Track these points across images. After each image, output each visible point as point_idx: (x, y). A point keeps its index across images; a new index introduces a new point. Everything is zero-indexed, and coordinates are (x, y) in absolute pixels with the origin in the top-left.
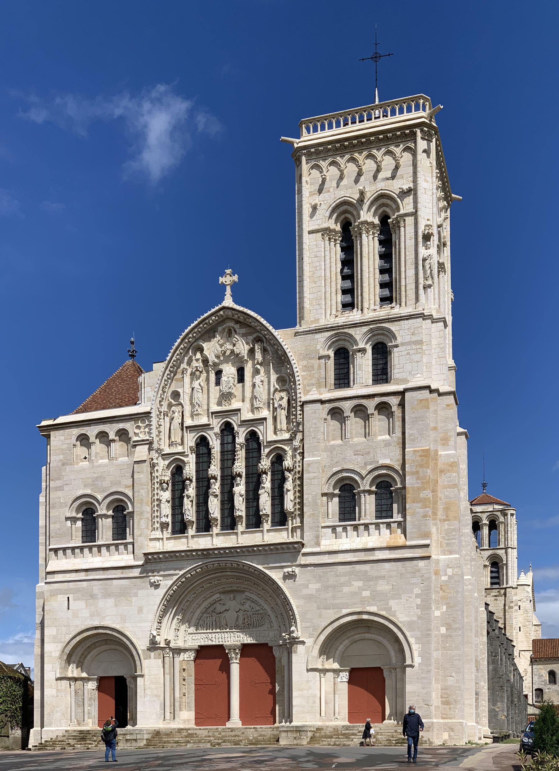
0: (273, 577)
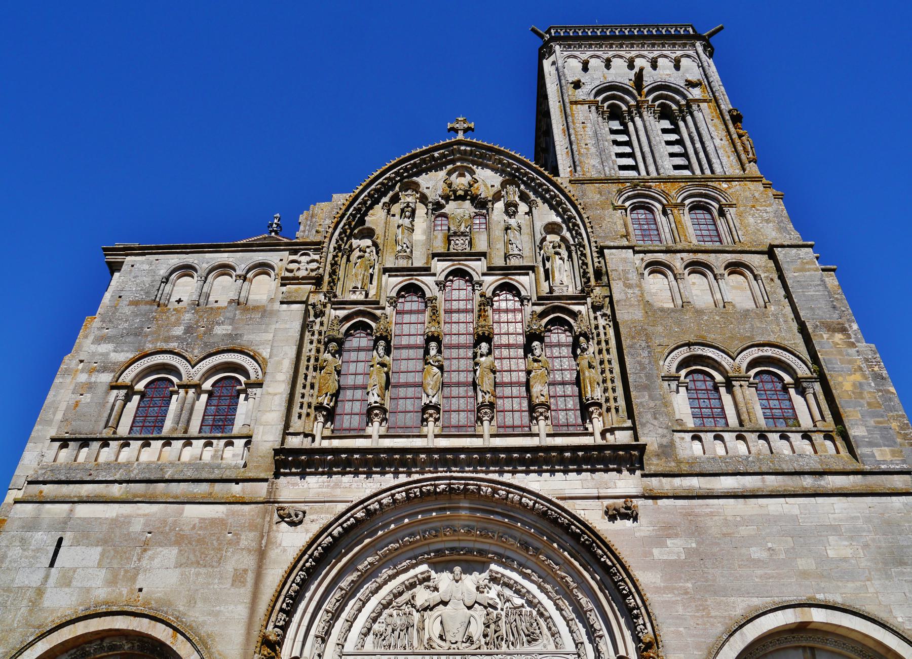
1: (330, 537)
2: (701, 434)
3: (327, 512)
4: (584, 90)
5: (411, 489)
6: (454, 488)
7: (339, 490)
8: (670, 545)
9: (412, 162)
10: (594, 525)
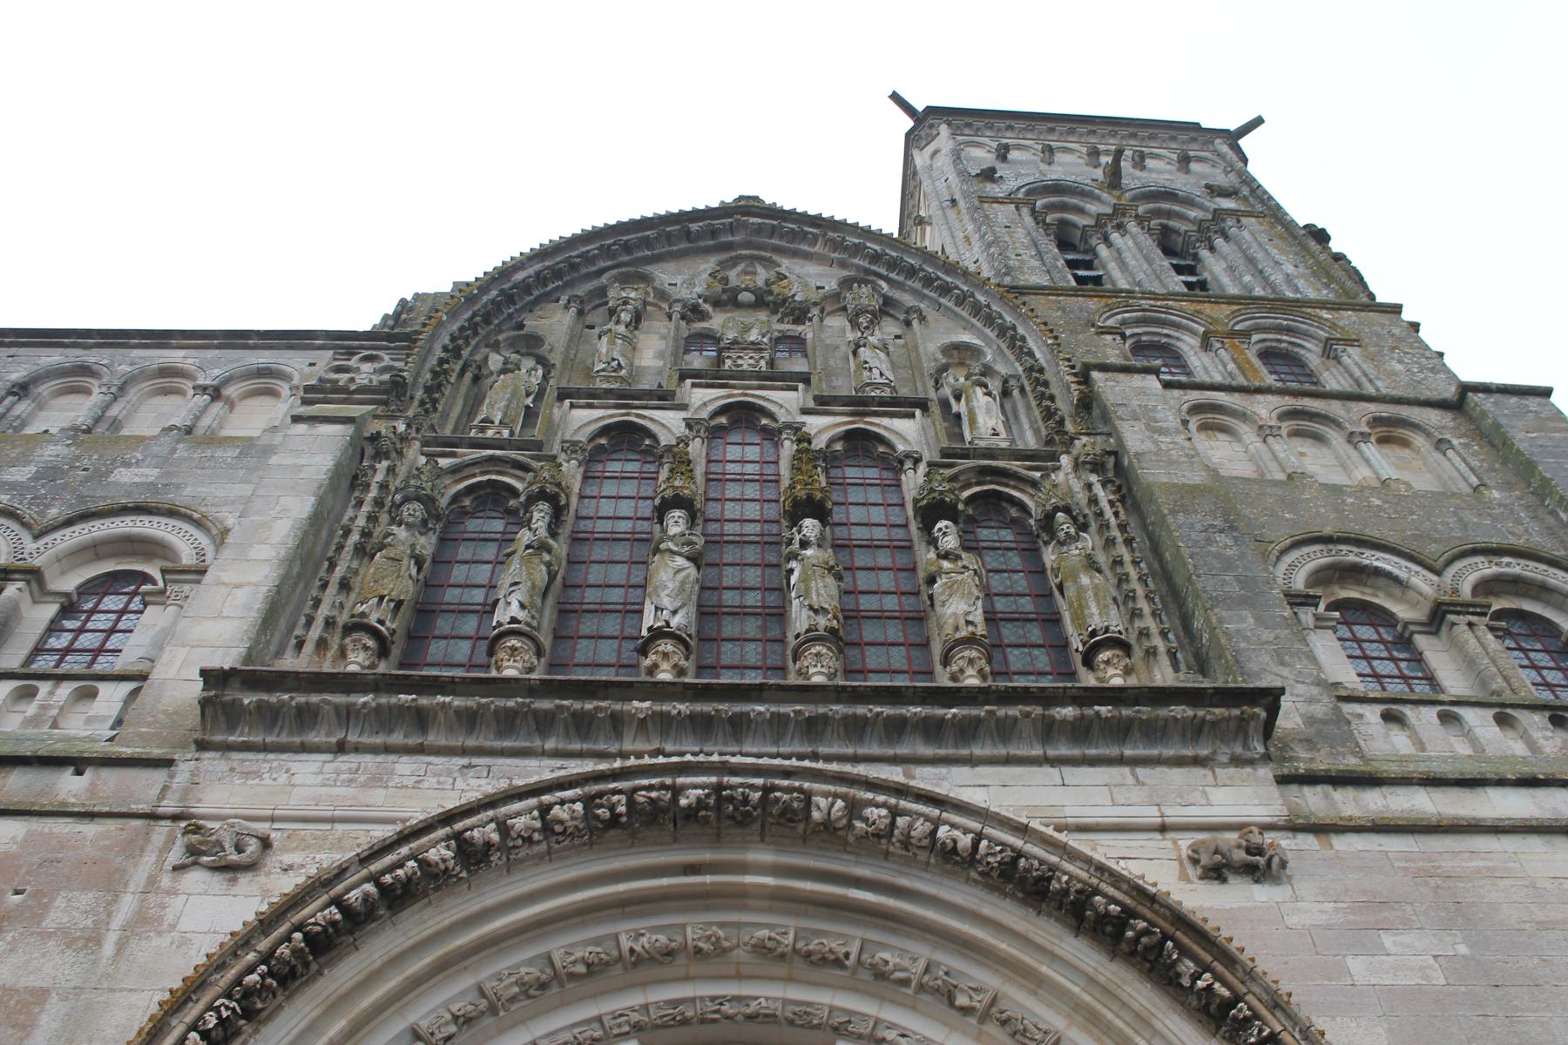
0: (1130, 869)
1: (333, 909)
2: (1408, 711)
3: (338, 845)
4: (1005, 187)
5: (600, 795)
6: (731, 799)
7: (381, 792)
8: (1393, 950)
9: (640, 235)
10: (1163, 888)
